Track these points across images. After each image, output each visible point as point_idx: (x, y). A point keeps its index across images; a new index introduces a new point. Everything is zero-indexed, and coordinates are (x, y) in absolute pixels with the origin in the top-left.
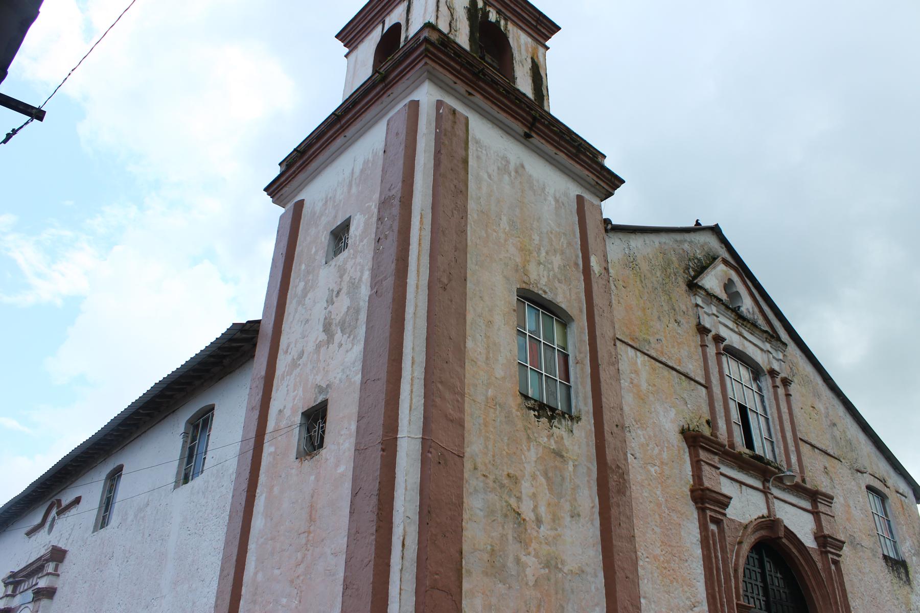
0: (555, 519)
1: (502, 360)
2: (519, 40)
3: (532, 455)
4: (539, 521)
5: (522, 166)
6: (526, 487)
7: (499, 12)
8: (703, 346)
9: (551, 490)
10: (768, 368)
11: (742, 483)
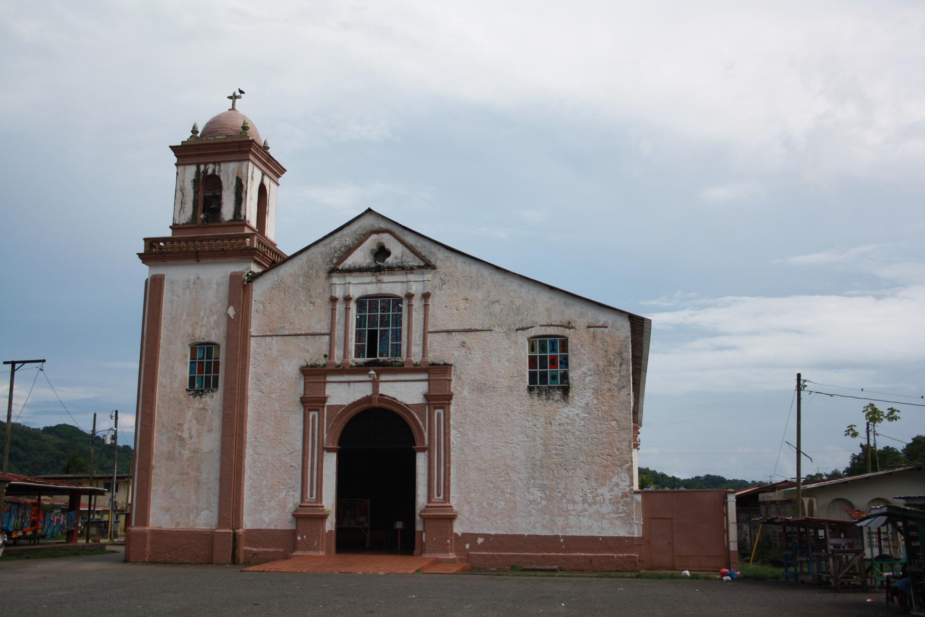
0: (199, 435)
1: (178, 380)
2: (227, 172)
3: (189, 414)
4: (191, 437)
5: (198, 278)
6: (186, 426)
7: (214, 163)
8: (333, 310)
9: (198, 423)
10: (405, 292)
11: (349, 382)
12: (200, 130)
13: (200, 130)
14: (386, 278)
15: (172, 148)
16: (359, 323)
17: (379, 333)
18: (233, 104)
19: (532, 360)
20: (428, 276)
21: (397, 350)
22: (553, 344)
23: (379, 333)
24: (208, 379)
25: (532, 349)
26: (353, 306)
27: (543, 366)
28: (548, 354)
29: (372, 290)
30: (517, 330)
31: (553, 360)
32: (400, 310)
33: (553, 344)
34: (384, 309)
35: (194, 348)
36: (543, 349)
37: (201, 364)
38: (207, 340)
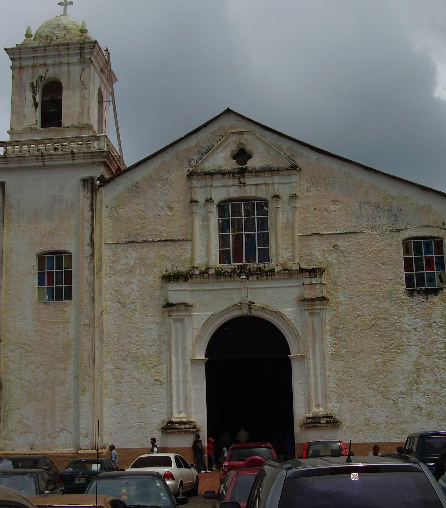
12: (33, 33)
13: (33, 33)
14: (250, 180)
15: (6, 50)
16: (223, 227)
17: (246, 237)
18: (65, 10)
19: (408, 264)
20: (295, 178)
21: (265, 256)
22: (428, 246)
23: (246, 237)
24: (59, 290)
25: (407, 251)
26: (214, 209)
27: (419, 268)
28: (424, 256)
29: (235, 193)
30: (392, 231)
31: (429, 261)
32: (266, 213)
33: (428, 246)
34: (247, 213)
35: (41, 258)
36: (418, 250)
37: (50, 274)
38: (57, 248)
